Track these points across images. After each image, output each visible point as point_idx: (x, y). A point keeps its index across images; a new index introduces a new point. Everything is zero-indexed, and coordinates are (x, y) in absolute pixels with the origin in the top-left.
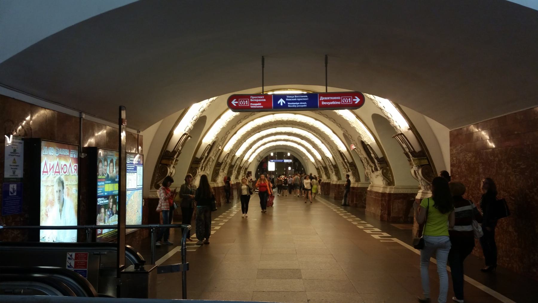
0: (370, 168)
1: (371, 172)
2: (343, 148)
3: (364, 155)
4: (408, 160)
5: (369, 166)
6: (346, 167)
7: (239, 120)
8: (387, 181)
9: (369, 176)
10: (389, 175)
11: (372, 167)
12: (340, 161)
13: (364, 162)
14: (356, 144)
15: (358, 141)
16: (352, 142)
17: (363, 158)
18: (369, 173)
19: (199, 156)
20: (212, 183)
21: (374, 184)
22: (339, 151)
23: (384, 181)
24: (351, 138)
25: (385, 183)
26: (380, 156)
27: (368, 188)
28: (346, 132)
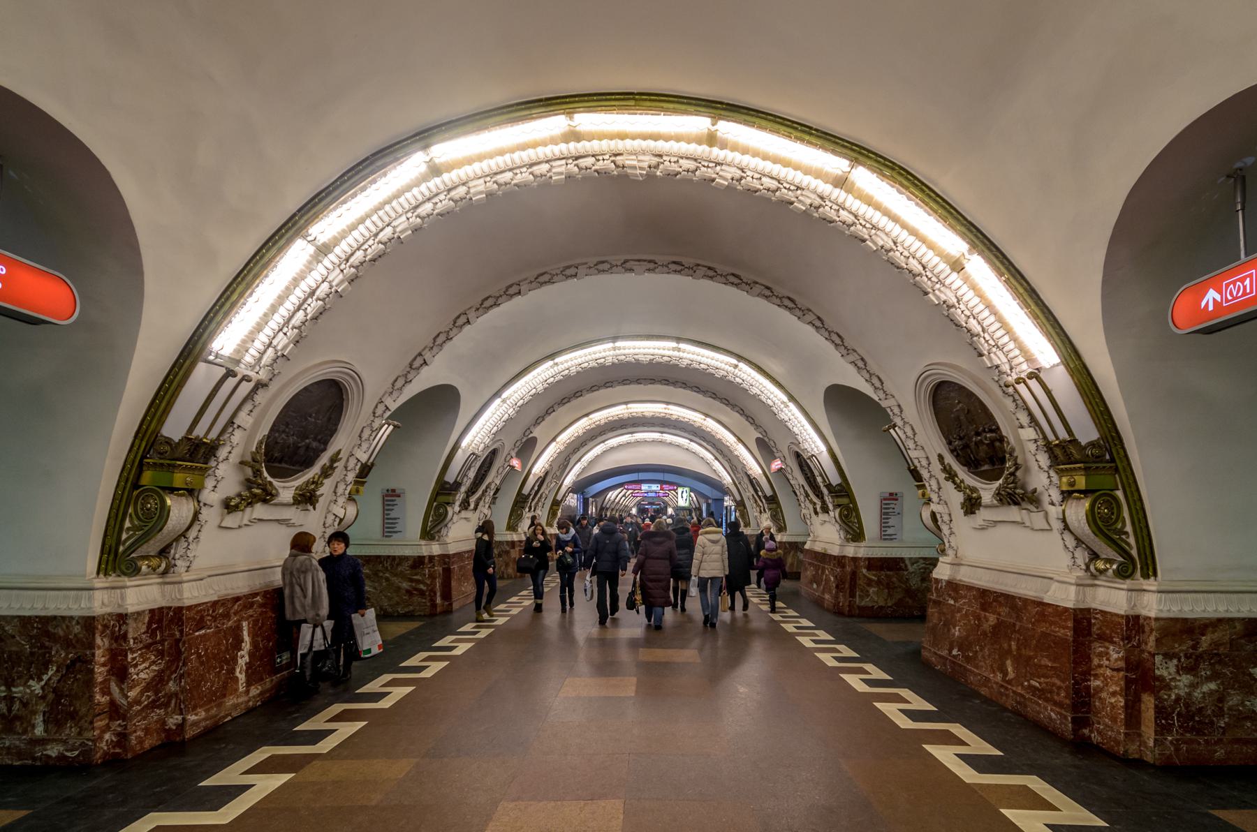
0: (811, 507)
1: (813, 514)
2: (755, 469)
3: (798, 479)
4: (918, 486)
5: (807, 501)
6: (761, 504)
7: (551, 405)
8: (847, 532)
9: (808, 522)
10: (852, 519)
11: (815, 504)
12: (749, 493)
13: (798, 494)
14: (783, 459)
15: (789, 453)
16: (777, 455)
17: (798, 487)
18: (808, 516)
19: (450, 477)
20: (508, 532)
21: (818, 537)
22: (748, 476)
23: (842, 533)
24: (773, 444)
25: (842, 537)
26: (835, 479)
27: (806, 543)
28: (764, 434)
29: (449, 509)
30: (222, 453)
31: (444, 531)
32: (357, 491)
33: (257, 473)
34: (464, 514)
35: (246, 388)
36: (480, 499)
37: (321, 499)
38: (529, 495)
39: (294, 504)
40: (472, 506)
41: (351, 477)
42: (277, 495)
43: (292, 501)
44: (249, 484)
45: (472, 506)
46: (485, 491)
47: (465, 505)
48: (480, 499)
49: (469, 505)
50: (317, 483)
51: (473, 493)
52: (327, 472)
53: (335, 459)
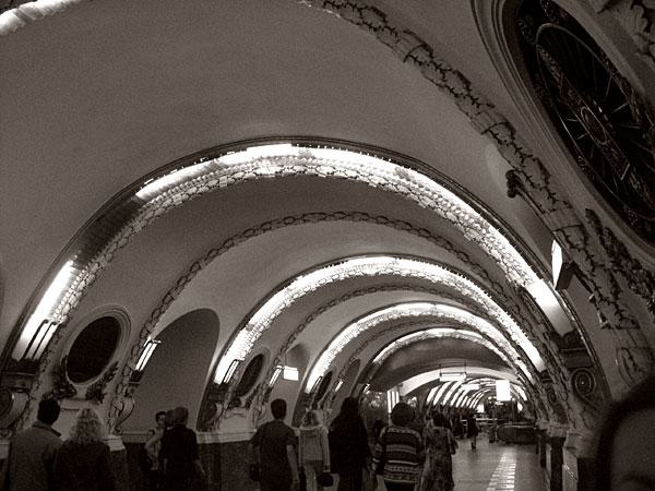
29: (219, 406)
30: (42, 368)
31: (216, 425)
32: (132, 391)
33: (63, 379)
34: (235, 410)
35: (54, 328)
36: (252, 397)
37: (106, 397)
38: (311, 394)
39: (87, 399)
40: (244, 403)
41: (126, 380)
42: (76, 392)
43: (84, 397)
44: (57, 385)
45: (244, 403)
46: (256, 391)
47: (235, 403)
48: (252, 397)
49: (240, 403)
50: (102, 385)
51: (245, 393)
52: (108, 378)
53: (114, 368)
